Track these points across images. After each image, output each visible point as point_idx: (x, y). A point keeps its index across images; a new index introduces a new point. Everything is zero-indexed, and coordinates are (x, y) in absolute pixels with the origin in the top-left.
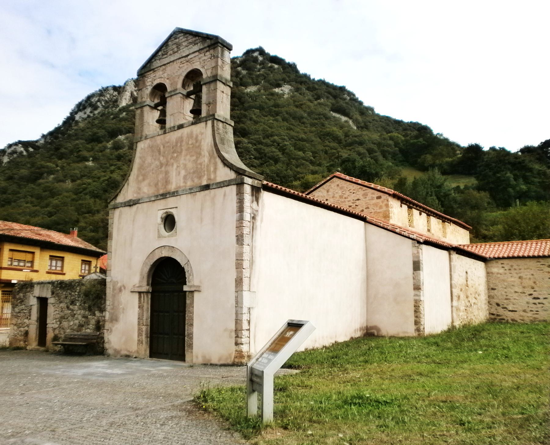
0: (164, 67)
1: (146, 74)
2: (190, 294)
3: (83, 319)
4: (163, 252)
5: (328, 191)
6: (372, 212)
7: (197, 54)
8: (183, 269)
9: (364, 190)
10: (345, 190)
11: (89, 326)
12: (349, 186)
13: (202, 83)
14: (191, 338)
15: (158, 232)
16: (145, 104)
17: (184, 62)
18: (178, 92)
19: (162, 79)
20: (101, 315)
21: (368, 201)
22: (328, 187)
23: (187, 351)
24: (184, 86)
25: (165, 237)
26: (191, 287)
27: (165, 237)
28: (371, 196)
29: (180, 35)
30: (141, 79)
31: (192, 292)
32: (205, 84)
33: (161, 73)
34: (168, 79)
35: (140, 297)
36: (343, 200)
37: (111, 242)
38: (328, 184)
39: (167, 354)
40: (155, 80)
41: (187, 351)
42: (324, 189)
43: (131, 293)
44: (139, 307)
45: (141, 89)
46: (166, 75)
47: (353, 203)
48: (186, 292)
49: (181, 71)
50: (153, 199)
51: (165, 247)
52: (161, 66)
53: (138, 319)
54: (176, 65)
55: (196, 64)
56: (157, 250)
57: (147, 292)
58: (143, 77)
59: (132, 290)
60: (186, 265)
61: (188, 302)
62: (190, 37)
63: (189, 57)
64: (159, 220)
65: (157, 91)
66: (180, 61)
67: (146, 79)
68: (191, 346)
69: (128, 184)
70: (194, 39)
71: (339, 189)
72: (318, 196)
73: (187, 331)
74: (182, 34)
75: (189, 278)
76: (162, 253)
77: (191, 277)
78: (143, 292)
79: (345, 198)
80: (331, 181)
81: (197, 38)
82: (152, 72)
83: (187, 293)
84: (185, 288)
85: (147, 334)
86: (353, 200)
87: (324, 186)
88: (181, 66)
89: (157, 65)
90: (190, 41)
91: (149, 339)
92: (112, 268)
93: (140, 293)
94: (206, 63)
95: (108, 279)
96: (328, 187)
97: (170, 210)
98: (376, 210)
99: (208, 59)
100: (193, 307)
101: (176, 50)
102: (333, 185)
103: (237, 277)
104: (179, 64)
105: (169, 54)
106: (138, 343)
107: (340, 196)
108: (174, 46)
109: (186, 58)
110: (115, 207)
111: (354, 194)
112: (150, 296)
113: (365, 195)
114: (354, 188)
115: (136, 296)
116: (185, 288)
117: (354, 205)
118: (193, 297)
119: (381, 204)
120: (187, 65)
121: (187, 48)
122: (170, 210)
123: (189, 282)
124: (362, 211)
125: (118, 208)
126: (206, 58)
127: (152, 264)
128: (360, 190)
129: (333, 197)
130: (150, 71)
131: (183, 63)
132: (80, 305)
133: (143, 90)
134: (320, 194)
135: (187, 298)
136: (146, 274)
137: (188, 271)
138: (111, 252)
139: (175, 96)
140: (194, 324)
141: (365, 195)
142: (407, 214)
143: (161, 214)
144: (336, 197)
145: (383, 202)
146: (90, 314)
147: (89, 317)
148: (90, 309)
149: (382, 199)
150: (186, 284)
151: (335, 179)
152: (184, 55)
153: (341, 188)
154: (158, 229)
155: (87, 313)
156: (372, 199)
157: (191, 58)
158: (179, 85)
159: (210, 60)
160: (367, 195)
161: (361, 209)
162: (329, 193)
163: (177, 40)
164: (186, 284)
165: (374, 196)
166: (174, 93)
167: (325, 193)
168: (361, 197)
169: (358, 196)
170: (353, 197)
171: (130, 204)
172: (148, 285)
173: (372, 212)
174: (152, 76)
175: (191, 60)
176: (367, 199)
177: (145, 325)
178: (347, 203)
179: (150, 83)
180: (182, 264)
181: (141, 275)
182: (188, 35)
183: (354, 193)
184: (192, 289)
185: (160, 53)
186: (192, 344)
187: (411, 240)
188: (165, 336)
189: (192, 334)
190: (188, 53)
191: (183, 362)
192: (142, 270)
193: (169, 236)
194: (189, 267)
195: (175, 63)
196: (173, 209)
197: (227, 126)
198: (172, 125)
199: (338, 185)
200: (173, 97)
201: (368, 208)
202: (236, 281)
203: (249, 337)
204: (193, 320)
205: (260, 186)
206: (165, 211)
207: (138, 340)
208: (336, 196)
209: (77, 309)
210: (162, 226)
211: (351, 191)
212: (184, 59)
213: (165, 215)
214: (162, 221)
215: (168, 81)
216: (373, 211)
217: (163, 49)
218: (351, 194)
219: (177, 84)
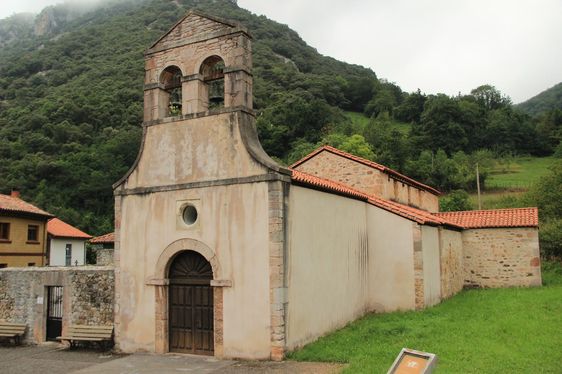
0: (177, 49)
1: (155, 54)
2: (218, 289)
3: (85, 311)
4: (184, 245)
5: (317, 164)
6: (363, 187)
7: (217, 40)
8: (208, 263)
9: (355, 165)
10: (335, 164)
11: (93, 319)
12: (340, 160)
13: (224, 72)
14: (221, 334)
15: (177, 223)
16: (156, 86)
17: (202, 47)
18: (196, 77)
21: (359, 176)
23: (216, 346)
24: (201, 71)
25: (186, 230)
26: (219, 282)
27: (186, 230)
28: (362, 171)
29: (195, 18)
30: (150, 58)
31: (221, 287)
32: (228, 73)
33: (174, 55)
34: (182, 62)
35: (157, 291)
36: (333, 174)
37: (118, 231)
38: (317, 156)
39: (190, 349)
40: (166, 62)
41: (216, 346)
44: (157, 301)
45: (150, 70)
46: (179, 58)
47: (343, 177)
48: (213, 287)
49: (198, 56)
50: (170, 189)
52: (173, 48)
53: (156, 313)
54: (192, 49)
55: (216, 50)
56: (176, 243)
57: (165, 286)
58: (151, 57)
60: (213, 259)
61: (216, 297)
63: (207, 42)
64: (178, 211)
65: (167, 73)
66: (197, 45)
67: (155, 59)
68: (220, 341)
69: (138, 171)
70: (212, 24)
72: (308, 169)
73: (216, 326)
74: (199, 17)
75: (216, 273)
76: (183, 246)
77: (218, 272)
78: (161, 286)
79: (335, 172)
80: (321, 154)
81: (217, 23)
82: (162, 53)
83: (215, 289)
84: (213, 283)
85: (165, 328)
86: (344, 174)
87: (313, 159)
88: (197, 50)
90: (208, 25)
91: (168, 333)
93: (157, 286)
94: (228, 51)
95: (117, 271)
98: (367, 186)
99: (230, 47)
100: (222, 302)
101: (191, 33)
102: (322, 158)
103: (272, 274)
104: (196, 48)
105: (182, 36)
107: (330, 169)
109: (204, 43)
110: (123, 195)
111: (344, 169)
112: (168, 289)
113: (356, 170)
114: (344, 163)
115: (154, 288)
116: (213, 283)
117: (345, 179)
118: (222, 292)
119: (372, 179)
120: (205, 50)
121: (204, 32)
123: (216, 277)
124: (353, 185)
125: (127, 195)
126: (227, 46)
127: (171, 256)
128: (351, 164)
129: (323, 170)
132: (80, 296)
133: (152, 70)
134: (309, 167)
135: (215, 293)
136: (164, 267)
137: (216, 265)
138: (119, 242)
139: (192, 82)
140: (224, 320)
141: (356, 170)
142: (393, 186)
143: (180, 204)
144: (326, 171)
145: (374, 177)
146: (93, 305)
147: (93, 309)
149: (373, 175)
150: (213, 279)
151: (324, 152)
153: (331, 162)
154: (177, 221)
155: (89, 304)
156: (364, 174)
157: (210, 44)
158: (197, 71)
159: (232, 48)
160: (358, 170)
161: (352, 183)
162: (319, 166)
163: (192, 23)
164: (213, 279)
165: (364, 171)
166: (189, 78)
167: (314, 166)
168: (352, 172)
169: (348, 170)
170: (343, 171)
171: (142, 192)
172: (166, 277)
173: (363, 187)
174: (163, 58)
175: (210, 46)
176: (358, 174)
177: (164, 320)
178: (337, 177)
180: (208, 258)
183: (344, 167)
184: (221, 285)
185: (171, 34)
187: (411, 222)
188: (187, 330)
189: (221, 329)
190: (206, 38)
191: (211, 357)
193: (190, 229)
194: (216, 261)
195: (191, 46)
196: (194, 201)
197: (251, 116)
198: (190, 112)
199: (328, 158)
200: (189, 82)
201: (358, 183)
202: (271, 277)
203: (284, 333)
205: (289, 181)
206: (185, 202)
207: (156, 335)
208: (326, 169)
209: (77, 300)
210: (181, 217)
211: (341, 165)
212: (201, 43)
213: (185, 206)
214: (181, 213)
215: (182, 64)
216: (364, 186)
217: (175, 30)
218: (341, 168)
219: (194, 69)
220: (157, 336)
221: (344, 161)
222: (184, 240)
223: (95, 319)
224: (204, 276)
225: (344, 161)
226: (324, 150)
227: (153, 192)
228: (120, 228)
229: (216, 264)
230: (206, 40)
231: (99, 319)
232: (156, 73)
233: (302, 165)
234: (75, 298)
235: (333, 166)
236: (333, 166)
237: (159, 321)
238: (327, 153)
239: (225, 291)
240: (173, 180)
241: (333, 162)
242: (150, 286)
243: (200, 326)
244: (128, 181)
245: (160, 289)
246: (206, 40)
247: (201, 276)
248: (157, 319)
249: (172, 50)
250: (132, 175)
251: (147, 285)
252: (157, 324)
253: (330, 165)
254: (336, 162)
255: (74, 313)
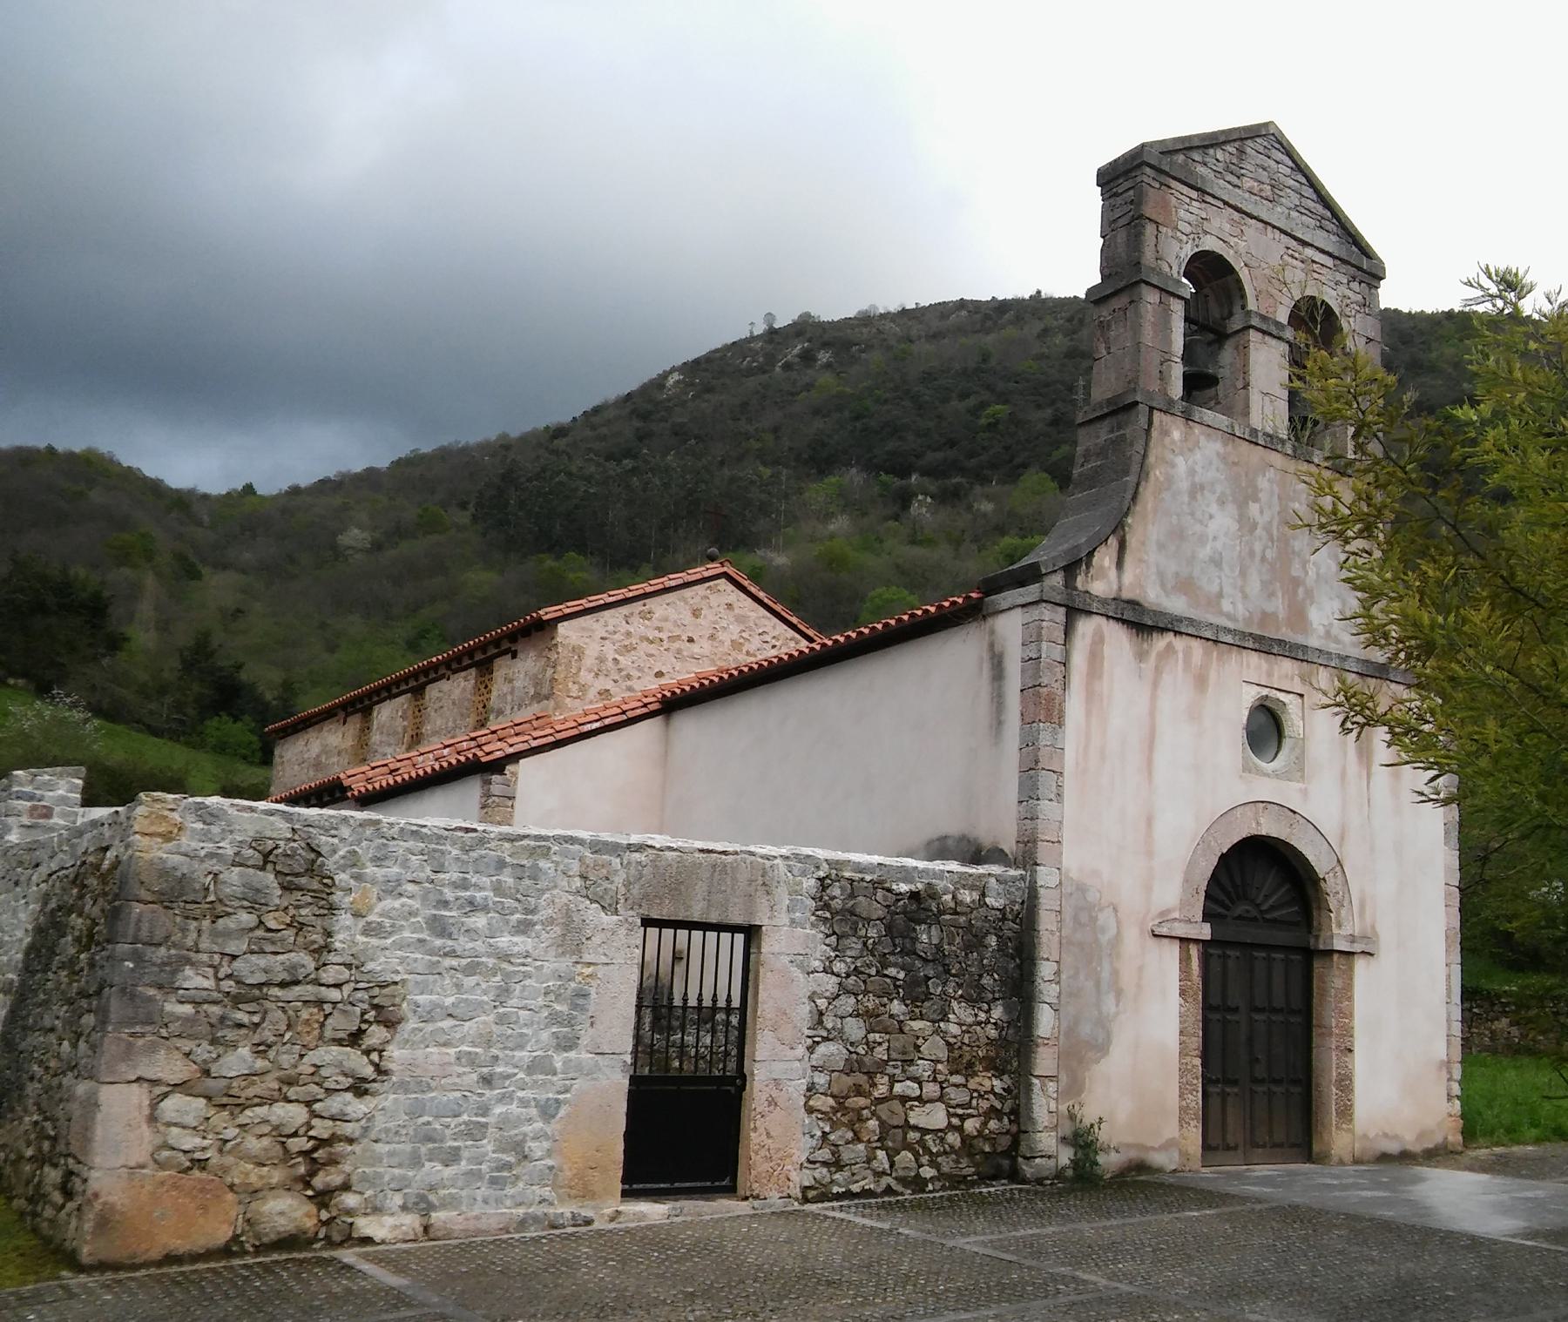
2: (1343, 960)
4: (1262, 820)
5: (696, 613)
7: (1329, 262)
10: (750, 629)
12: (766, 622)
17: (1296, 255)
19: (1232, 252)
20: (982, 1016)
22: (697, 599)
31: (1349, 954)
35: (1185, 960)
37: (1055, 732)
38: (700, 590)
42: (685, 600)
43: (1152, 942)
50: (1229, 639)
51: (1269, 806)
52: (1226, 203)
59: (1164, 931)
62: (1308, 192)
63: (1309, 252)
68: (1346, 1112)
71: (732, 619)
72: (666, 620)
74: (1290, 163)
75: (1338, 913)
76: (1258, 823)
77: (1343, 912)
78: (1196, 941)
80: (711, 583)
87: (687, 593)
89: (1219, 193)
90: (1311, 204)
92: (1067, 835)
93: (1184, 941)
96: (697, 599)
97: (1282, 696)
101: (1267, 190)
102: (715, 600)
106: (1181, 1120)
108: (1264, 176)
109: (1300, 248)
118: (1351, 969)
122: (1282, 696)
123: (1339, 926)
129: (712, 637)
130: (1197, 189)
131: (1292, 256)
137: (1338, 893)
140: (1356, 1049)
143: (1250, 695)
147: (917, 1025)
148: (915, 993)
152: (1300, 236)
153: (740, 619)
155: (897, 1007)
167: (687, 617)
179: (1188, 229)
181: (1186, 881)
182: (1304, 180)
183: (774, 647)
186: (1351, 1105)
192: (1191, 864)
199: (729, 606)
204: (1352, 1036)
206: (1265, 692)
208: (721, 636)
220: (1183, 1110)
221: (774, 627)
222: (1261, 805)
223: (922, 1068)
224: (1275, 921)
225: (774, 627)
226: (725, 575)
227: (1177, 633)
228: (1061, 725)
229: (1339, 888)
230: (1304, 243)
231: (940, 1067)
232: (1175, 245)
233: (652, 603)
234: (830, 984)
235: (744, 634)
236: (744, 634)
237: (1189, 1059)
238: (730, 587)
239: (1360, 964)
240: (1235, 610)
241: (743, 622)
242: (1166, 941)
243: (1260, 1071)
244: (1089, 565)
245: (1194, 951)
246: (1304, 243)
247: (1268, 921)
248: (1182, 1054)
249: (1220, 204)
250: (1102, 549)
251: (1155, 936)
252: (1183, 1071)
253: (735, 629)
254: (752, 624)
255: (822, 1049)
